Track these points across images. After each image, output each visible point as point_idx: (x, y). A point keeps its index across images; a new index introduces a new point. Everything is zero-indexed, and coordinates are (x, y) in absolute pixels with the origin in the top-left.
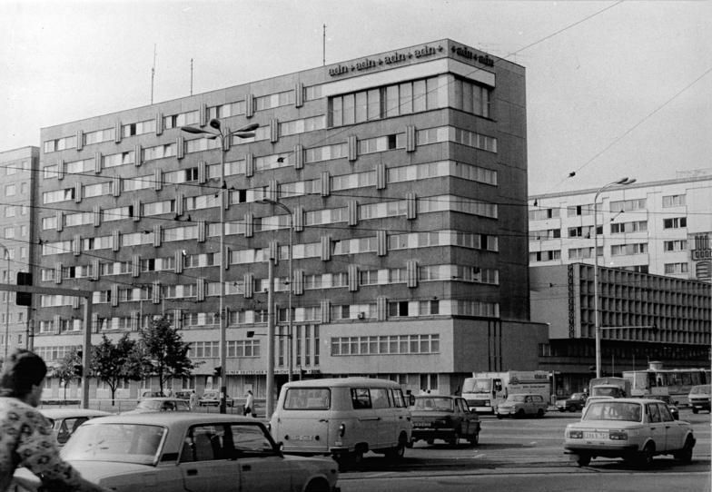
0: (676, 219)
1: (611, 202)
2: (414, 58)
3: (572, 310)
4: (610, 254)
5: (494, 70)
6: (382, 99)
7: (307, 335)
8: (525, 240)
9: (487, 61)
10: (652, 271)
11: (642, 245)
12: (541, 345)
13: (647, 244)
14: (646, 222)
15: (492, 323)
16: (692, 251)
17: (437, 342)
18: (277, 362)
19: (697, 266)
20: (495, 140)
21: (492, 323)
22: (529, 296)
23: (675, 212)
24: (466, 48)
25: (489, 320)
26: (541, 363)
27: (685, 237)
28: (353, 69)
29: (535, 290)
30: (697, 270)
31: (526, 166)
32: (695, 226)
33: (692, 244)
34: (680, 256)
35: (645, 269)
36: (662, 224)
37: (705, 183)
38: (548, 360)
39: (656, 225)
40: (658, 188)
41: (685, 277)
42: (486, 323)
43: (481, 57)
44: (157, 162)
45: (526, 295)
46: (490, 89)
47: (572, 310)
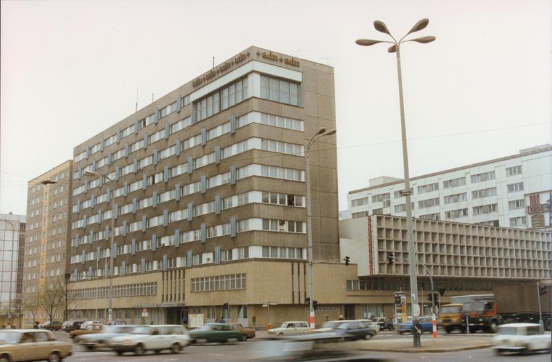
0: (516, 184)
1: (472, 176)
2: (235, 64)
3: (371, 252)
4: (472, 214)
5: (301, 69)
6: (220, 99)
7: (167, 276)
8: (335, 199)
9: (292, 63)
10: (501, 225)
11: (494, 205)
12: (349, 282)
13: (497, 204)
14: (495, 188)
15: (296, 265)
16: (528, 207)
17: (245, 280)
18: (165, 299)
19: (532, 218)
20: (302, 123)
21: (296, 265)
22: (338, 243)
23: (515, 179)
24: (271, 52)
25: (292, 262)
26: (348, 296)
27: (522, 198)
28: (204, 80)
29: (345, 237)
30: (532, 221)
31: (336, 142)
32: (529, 189)
33: (528, 203)
34: (521, 212)
35: (496, 223)
36: (506, 189)
37: (547, 153)
38: (358, 293)
39: (502, 191)
40: (502, 163)
41: (524, 228)
42: (289, 264)
43: (287, 60)
44: (118, 161)
45: (335, 241)
46: (298, 83)
47: (371, 252)
